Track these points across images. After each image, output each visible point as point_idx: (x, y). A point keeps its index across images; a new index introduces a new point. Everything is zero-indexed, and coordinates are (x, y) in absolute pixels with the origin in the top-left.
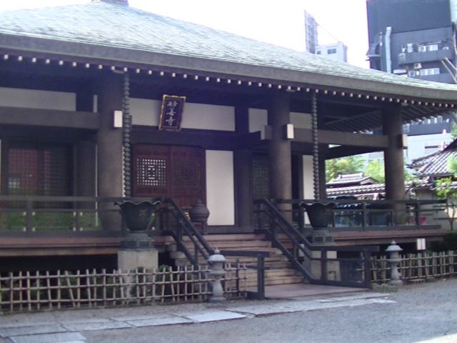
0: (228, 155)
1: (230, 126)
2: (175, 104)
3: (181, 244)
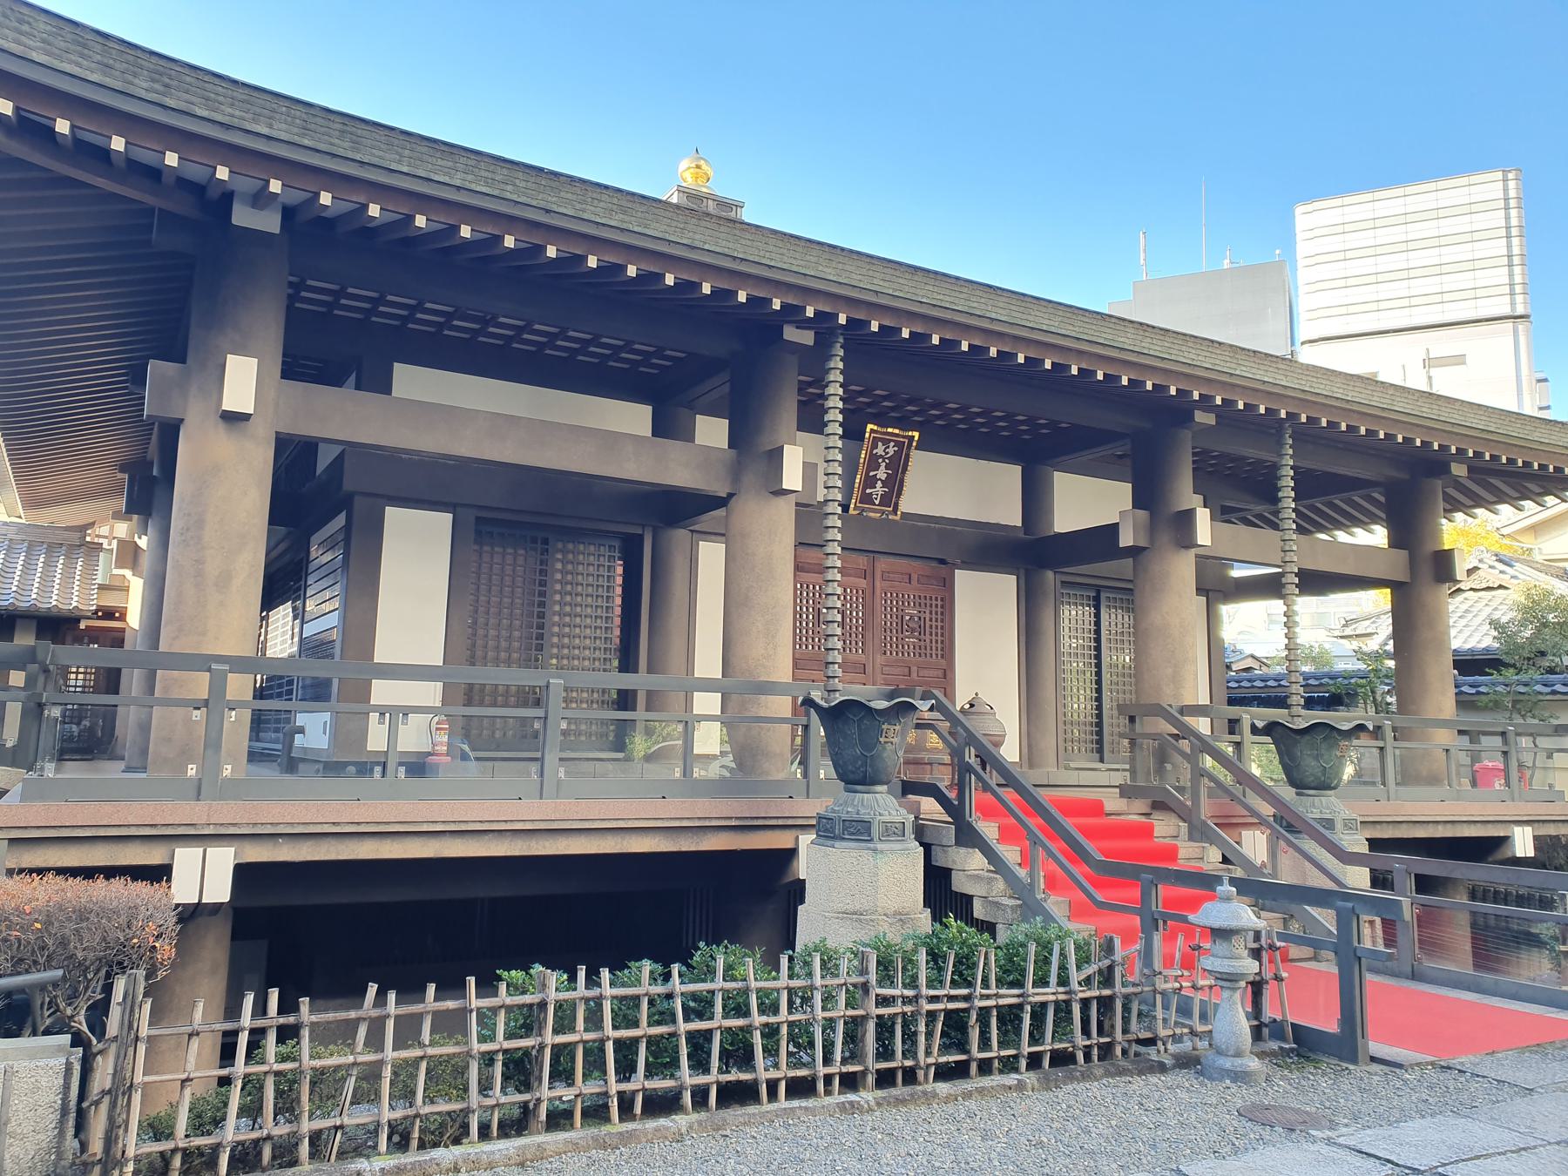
0: (1006, 584)
1: (1010, 514)
2: (891, 451)
3: (970, 825)
